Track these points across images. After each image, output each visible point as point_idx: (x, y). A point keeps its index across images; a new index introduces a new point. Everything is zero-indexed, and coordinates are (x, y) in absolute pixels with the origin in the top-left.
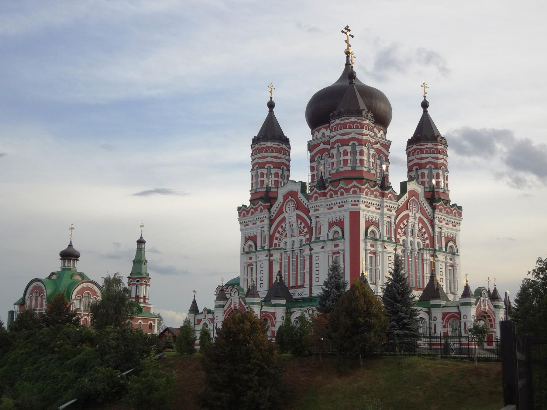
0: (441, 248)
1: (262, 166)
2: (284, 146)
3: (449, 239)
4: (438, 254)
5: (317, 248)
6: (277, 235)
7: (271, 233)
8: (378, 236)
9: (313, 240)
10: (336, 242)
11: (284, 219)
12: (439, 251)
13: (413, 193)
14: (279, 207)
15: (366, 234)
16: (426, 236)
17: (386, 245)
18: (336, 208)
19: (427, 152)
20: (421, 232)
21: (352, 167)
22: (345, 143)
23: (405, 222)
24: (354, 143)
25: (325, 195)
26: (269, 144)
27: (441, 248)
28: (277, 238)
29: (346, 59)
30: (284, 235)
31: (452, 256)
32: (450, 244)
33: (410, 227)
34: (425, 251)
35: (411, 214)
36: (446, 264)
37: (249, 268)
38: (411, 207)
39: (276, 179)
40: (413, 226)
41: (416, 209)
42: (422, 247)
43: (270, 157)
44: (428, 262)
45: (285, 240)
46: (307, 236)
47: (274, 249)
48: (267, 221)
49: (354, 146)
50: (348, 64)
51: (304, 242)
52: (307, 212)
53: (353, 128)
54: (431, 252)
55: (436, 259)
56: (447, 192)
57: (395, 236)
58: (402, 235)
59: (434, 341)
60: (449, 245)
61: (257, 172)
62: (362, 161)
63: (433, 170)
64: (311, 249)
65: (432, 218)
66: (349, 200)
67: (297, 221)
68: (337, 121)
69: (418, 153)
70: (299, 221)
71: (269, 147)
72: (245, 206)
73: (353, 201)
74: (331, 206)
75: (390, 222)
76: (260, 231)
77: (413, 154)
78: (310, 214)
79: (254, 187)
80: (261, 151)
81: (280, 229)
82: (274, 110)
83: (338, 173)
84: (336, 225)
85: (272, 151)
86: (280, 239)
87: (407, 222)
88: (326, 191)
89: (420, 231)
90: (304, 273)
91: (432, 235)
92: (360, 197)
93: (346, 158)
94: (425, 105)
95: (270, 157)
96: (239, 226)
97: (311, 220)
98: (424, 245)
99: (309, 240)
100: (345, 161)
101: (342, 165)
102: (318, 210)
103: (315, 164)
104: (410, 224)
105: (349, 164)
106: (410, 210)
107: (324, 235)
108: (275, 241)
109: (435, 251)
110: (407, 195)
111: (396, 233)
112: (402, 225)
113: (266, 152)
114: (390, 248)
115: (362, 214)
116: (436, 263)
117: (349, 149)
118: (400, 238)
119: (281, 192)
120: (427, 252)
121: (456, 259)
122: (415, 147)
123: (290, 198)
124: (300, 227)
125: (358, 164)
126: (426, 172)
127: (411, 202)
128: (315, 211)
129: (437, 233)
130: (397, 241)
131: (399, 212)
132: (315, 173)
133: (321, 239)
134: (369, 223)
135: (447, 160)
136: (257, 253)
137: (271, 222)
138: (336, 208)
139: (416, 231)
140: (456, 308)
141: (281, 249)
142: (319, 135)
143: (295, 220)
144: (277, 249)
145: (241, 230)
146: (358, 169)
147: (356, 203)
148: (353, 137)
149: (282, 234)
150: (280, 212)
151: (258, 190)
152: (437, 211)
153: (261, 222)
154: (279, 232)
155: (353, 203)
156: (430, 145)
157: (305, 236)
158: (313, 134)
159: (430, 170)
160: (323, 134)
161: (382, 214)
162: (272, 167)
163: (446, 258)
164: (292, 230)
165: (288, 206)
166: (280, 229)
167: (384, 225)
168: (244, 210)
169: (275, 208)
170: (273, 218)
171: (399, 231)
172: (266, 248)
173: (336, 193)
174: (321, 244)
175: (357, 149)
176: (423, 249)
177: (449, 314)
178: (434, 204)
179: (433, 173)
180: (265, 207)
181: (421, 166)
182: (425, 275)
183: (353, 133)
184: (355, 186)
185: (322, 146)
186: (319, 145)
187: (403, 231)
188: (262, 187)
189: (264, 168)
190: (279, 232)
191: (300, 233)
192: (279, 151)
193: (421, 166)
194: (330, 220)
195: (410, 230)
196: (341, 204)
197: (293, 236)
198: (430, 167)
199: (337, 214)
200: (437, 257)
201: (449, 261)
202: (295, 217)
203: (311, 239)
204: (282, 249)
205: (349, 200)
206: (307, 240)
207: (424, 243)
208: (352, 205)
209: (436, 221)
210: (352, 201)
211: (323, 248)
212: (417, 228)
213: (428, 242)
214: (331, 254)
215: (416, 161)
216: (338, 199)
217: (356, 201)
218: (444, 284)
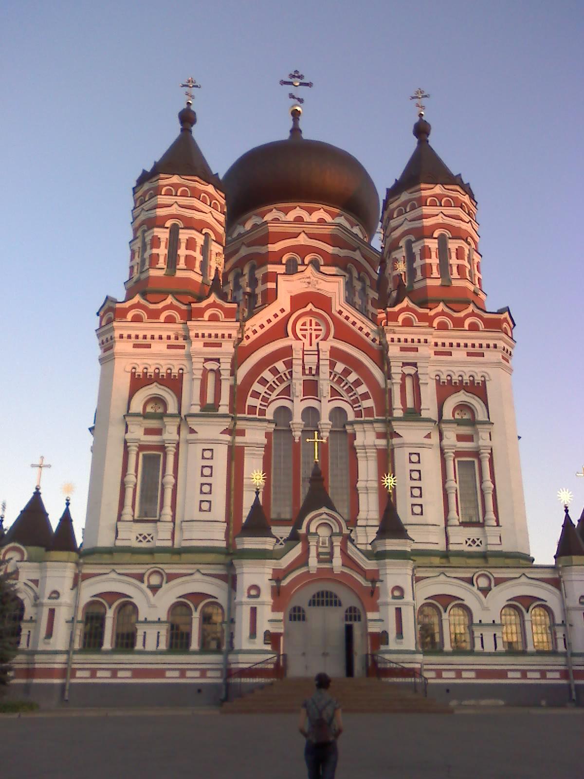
0: (413, 414)
4: (397, 427)
24: (175, 224)
44: (373, 454)
49: (174, 231)
53: (176, 195)
54: (379, 427)
63: (450, 241)
92: (113, 329)
98: (358, 414)
109: (388, 423)
116: (397, 452)
120: (364, 428)
121: (480, 434)
134: (138, 382)
148: (175, 213)
159: (442, 240)
161: (189, 357)
167: (193, 379)
176: (352, 423)
179: (450, 246)
198: (442, 235)
200: (399, 436)
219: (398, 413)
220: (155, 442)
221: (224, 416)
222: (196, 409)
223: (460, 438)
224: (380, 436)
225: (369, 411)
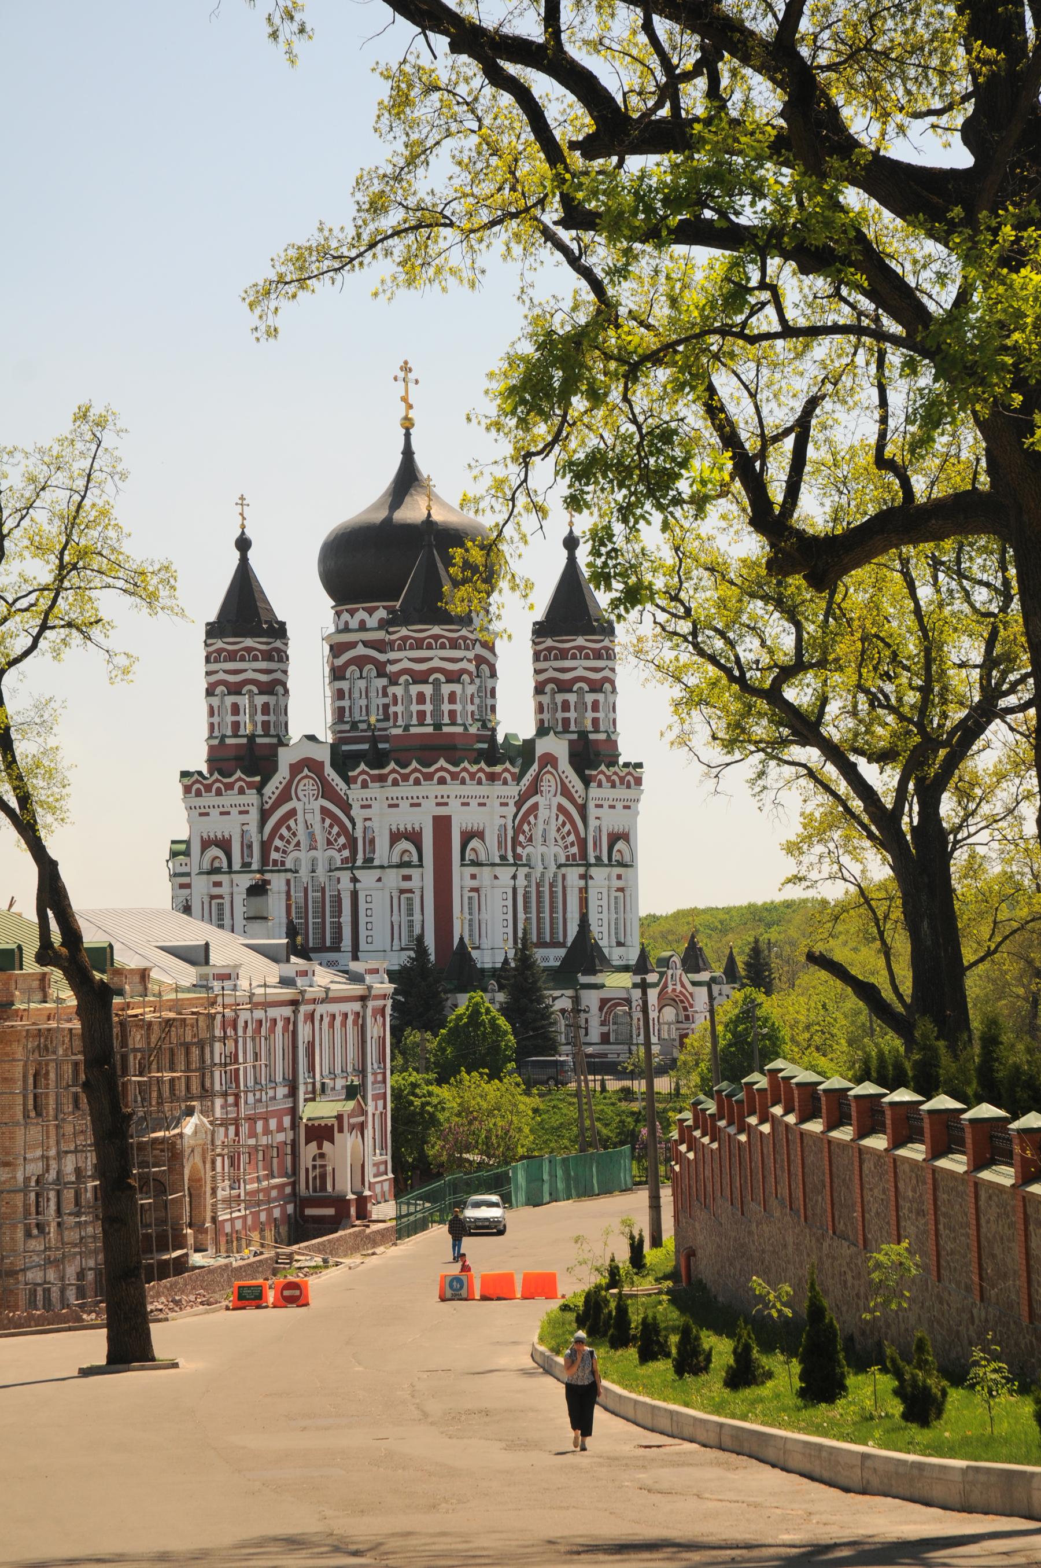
0: (598, 858)
1: (235, 689)
2: (278, 644)
3: (614, 838)
4: (594, 871)
5: (368, 879)
6: (277, 842)
7: (265, 838)
8: (483, 857)
9: (359, 863)
10: (406, 871)
11: (293, 813)
12: (596, 865)
13: (550, 760)
14: (281, 787)
15: (463, 858)
17: (498, 870)
18: (404, 805)
19: (574, 657)
22: (420, 678)
25: (382, 779)
26: (249, 642)
27: (598, 858)
28: (277, 849)
29: (403, 438)
30: (294, 843)
32: (620, 845)
34: (569, 869)
37: (214, 902)
39: (266, 718)
40: (547, 822)
41: (553, 789)
42: (563, 861)
43: (252, 670)
44: (576, 891)
45: (296, 854)
46: (346, 853)
47: (272, 871)
48: (254, 816)
49: (437, 684)
50: (408, 453)
51: (338, 864)
52: (346, 808)
54: (582, 870)
56: (613, 737)
57: (514, 850)
60: (616, 848)
61: (222, 701)
64: (355, 880)
66: (432, 796)
67: (323, 820)
68: (404, 632)
69: (556, 658)
70: (328, 821)
71: (248, 650)
72: (200, 773)
74: (395, 802)
76: (239, 831)
77: (546, 659)
78: (353, 813)
79: (216, 733)
80: (232, 657)
81: (284, 831)
82: (250, 554)
83: (407, 736)
84: (407, 839)
85: (255, 659)
86: (284, 852)
87: (536, 817)
88: (385, 771)
89: (559, 830)
90: (340, 923)
91: (583, 835)
93: (421, 707)
95: (252, 670)
96: (185, 814)
97: (354, 824)
99: (350, 864)
100: (422, 715)
101: (414, 721)
102: (369, 806)
103: (344, 685)
104: (540, 820)
105: (429, 720)
107: (382, 853)
108: (274, 855)
110: (535, 766)
111: (515, 842)
112: (526, 827)
113: (242, 659)
114: (505, 874)
117: (428, 689)
119: (286, 758)
122: (549, 642)
123: (306, 771)
124: (330, 833)
125: (446, 720)
126: (572, 698)
128: (363, 807)
129: (591, 829)
130: (517, 857)
131: (519, 805)
132: (346, 703)
133: (376, 863)
136: (233, 876)
137: (264, 816)
138: (404, 805)
139: (553, 833)
141: (286, 871)
142: (354, 624)
143: (318, 816)
144: (279, 871)
145: (189, 821)
147: (445, 800)
149: (288, 842)
150: (285, 796)
151: (228, 741)
153: (241, 813)
154: (282, 838)
155: (439, 800)
156: (580, 641)
157: (339, 851)
158: (338, 614)
160: (362, 623)
162: (256, 691)
164: (312, 836)
165: (301, 787)
166: (284, 831)
168: (197, 781)
169: (272, 789)
170: (267, 807)
171: (521, 838)
172: (255, 867)
173: (405, 778)
174: (377, 873)
178: (587, 772)
180: (250, 785)
181: (564, 687)
182: (569, 915)
183: (436, 660)
184: (442, 769)
185: (361, 650)
186: (353, 645)
188: (236, 735)
189: (239, 693)
190: (282, 838)
191: (329, 843)
192: (268, 656)
193: (564, 687)
194: (394, 829)
195: (540, 833)
196: (415, 801)
197: (313, 848)
199: (406, 818)
200: (591, 878)
202: (318, 812)
203: (354, 860)
204: (290, 870)
205: (432, 796)
206: (344, 861)
208: (438, 804)
209: (591, 805)
211: (379, 880)
212: (554, 828)
213: (575, 850)
214: (395, 894)
215: (551, 674)
216: (407, 790)
218: (605, 929)
219: (592, 861)
223: (619, 877)
225: (574, 855)
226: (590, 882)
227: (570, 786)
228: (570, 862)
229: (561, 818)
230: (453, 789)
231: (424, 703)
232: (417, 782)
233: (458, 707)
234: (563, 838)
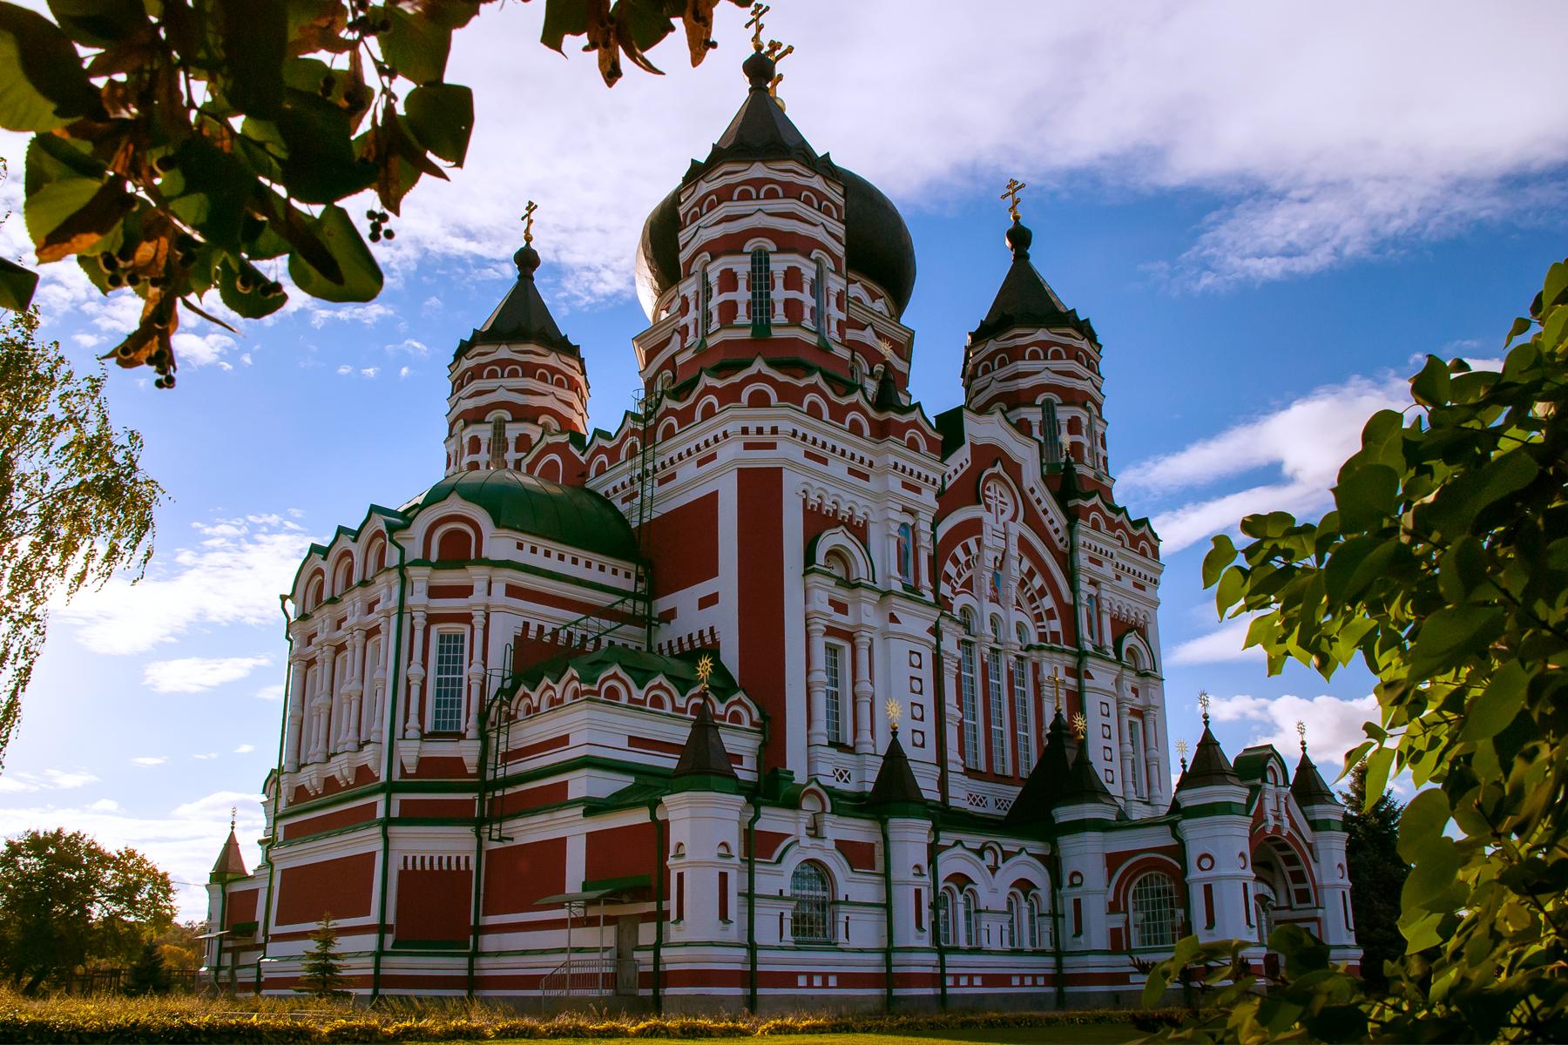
0: (1099, 648)
4: (1092, 664)
12: (1094, 656)
16: (1048, 602)
20: (1029, 589)
21: (754, 326)
23: (971, 542)
31: (1138, 680)
32: (1130, 640)
33: (989, 556)
35: (988, 518)
36: (1119, 703)
38: (990, 498)
40: (1001, 563)
42: (1034, 640)
54: (1070, 661)
55: (1087, 682)
58: (958, 590)
59: (1073, 965)
62: (793, 308)
65: (1068, 549)
66: (733, 427)
73: (752, 429)
75: (909, 530)
89: (1023, 584)
94: (1020, 238)
98: (1042, 637)
104: (989, 556)
105: (742, 317)
106: (988, 508)
115: (792, 486)
118: (952, 599)
125: (779, 317)
127: (990, 484)
129: (1084, 596)
130: (942, 603)
135: (1101, 405)
140: (1167, 829)
146: (776, 333)
147: (767, 437)
152: (1082, 526)
155: (753, 437)
163: (1118, 682)
171: (949, 568)
175: (772, 267)
177: (1133, 856)
184: (760, 377)
187: (965, 576)
196: (705, 452)
198: (1047, 403)
200: (1089, 676)
201: (1130, 695)
207: (1041, 630)
208: (748, 446)
209: (1082, 559)
210: (745, 431)
213: (1056, 625)
217: (767, 429)
220: (847, 626)
221: (928, 604)
222: (897, 586)
224: (1070, 672)
225: (1055, 635)
226: (1087, 682)
227: (1039, 509)
228: (1047, 643)
229: (1027, 564)
230: (783, 418)
231: (735, 288)
232: (709, 412)
233: (809, 301)
234: (1032, 599)
